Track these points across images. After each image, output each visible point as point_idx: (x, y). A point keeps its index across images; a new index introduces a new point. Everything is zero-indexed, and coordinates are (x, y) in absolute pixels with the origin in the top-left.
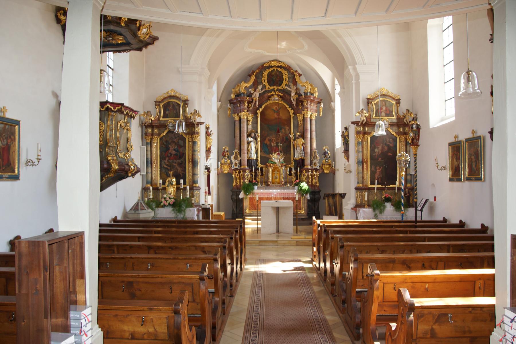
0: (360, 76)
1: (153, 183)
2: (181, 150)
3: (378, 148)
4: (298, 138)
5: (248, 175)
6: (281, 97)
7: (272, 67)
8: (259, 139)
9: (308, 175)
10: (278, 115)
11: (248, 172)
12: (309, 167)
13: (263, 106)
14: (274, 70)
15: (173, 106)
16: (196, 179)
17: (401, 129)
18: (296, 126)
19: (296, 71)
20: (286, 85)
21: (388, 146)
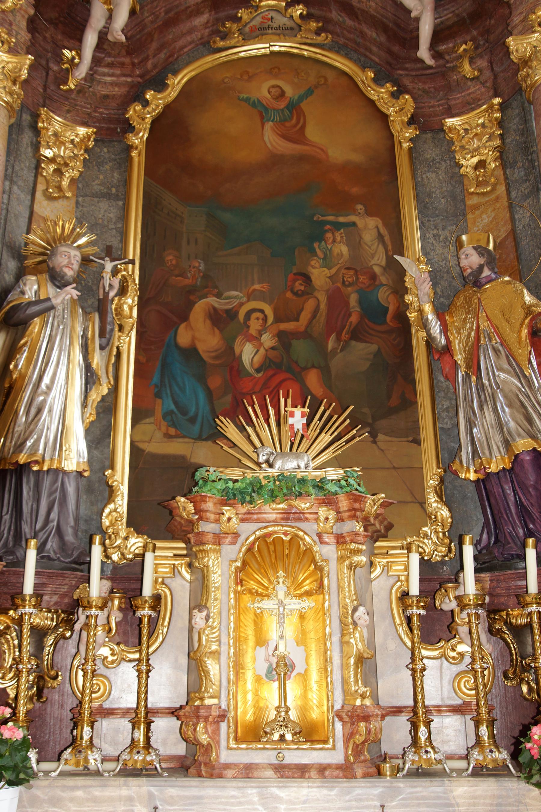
8: (130, 304)
13: (177, 82)
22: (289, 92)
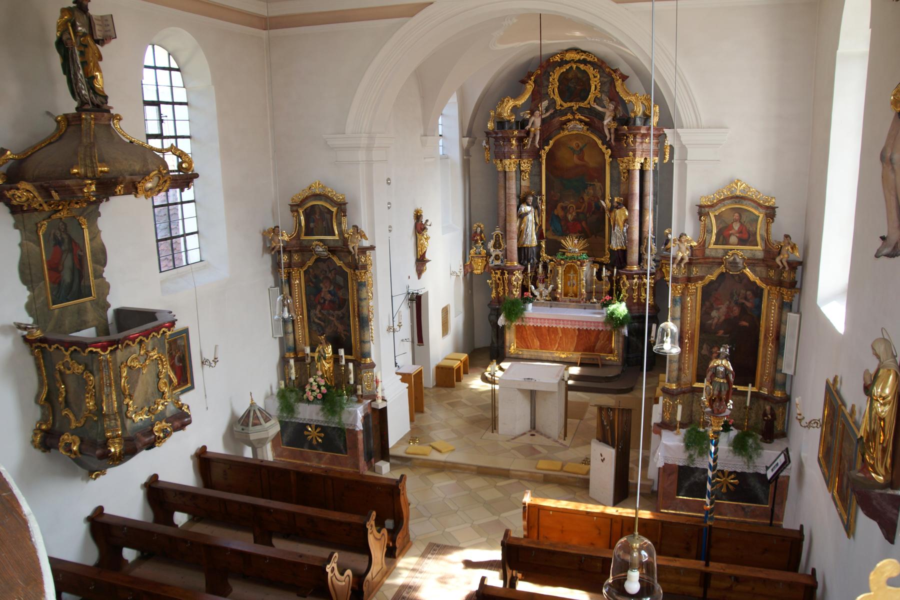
0: (689, 150)
1: (298, 349)
2: (340, 294)
3: (718, 309)
4: (617, 208)
5: (517, 280)
6: (586, 124)
7: (567, 62)
9: (631, 284)
10: (582, 159)
11: (518, 275)
12: (635, 268)
13: (551, 142)
14: (571, 67)
15: (321, 213)
16: (366, 350)
17: (772, 273)
18: (615, 182)
19: (615, 71)
20: (596, 100)
21: (743, 307)
22: (581, 145)
